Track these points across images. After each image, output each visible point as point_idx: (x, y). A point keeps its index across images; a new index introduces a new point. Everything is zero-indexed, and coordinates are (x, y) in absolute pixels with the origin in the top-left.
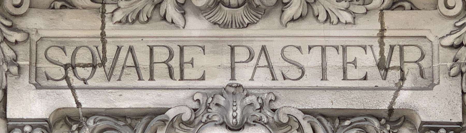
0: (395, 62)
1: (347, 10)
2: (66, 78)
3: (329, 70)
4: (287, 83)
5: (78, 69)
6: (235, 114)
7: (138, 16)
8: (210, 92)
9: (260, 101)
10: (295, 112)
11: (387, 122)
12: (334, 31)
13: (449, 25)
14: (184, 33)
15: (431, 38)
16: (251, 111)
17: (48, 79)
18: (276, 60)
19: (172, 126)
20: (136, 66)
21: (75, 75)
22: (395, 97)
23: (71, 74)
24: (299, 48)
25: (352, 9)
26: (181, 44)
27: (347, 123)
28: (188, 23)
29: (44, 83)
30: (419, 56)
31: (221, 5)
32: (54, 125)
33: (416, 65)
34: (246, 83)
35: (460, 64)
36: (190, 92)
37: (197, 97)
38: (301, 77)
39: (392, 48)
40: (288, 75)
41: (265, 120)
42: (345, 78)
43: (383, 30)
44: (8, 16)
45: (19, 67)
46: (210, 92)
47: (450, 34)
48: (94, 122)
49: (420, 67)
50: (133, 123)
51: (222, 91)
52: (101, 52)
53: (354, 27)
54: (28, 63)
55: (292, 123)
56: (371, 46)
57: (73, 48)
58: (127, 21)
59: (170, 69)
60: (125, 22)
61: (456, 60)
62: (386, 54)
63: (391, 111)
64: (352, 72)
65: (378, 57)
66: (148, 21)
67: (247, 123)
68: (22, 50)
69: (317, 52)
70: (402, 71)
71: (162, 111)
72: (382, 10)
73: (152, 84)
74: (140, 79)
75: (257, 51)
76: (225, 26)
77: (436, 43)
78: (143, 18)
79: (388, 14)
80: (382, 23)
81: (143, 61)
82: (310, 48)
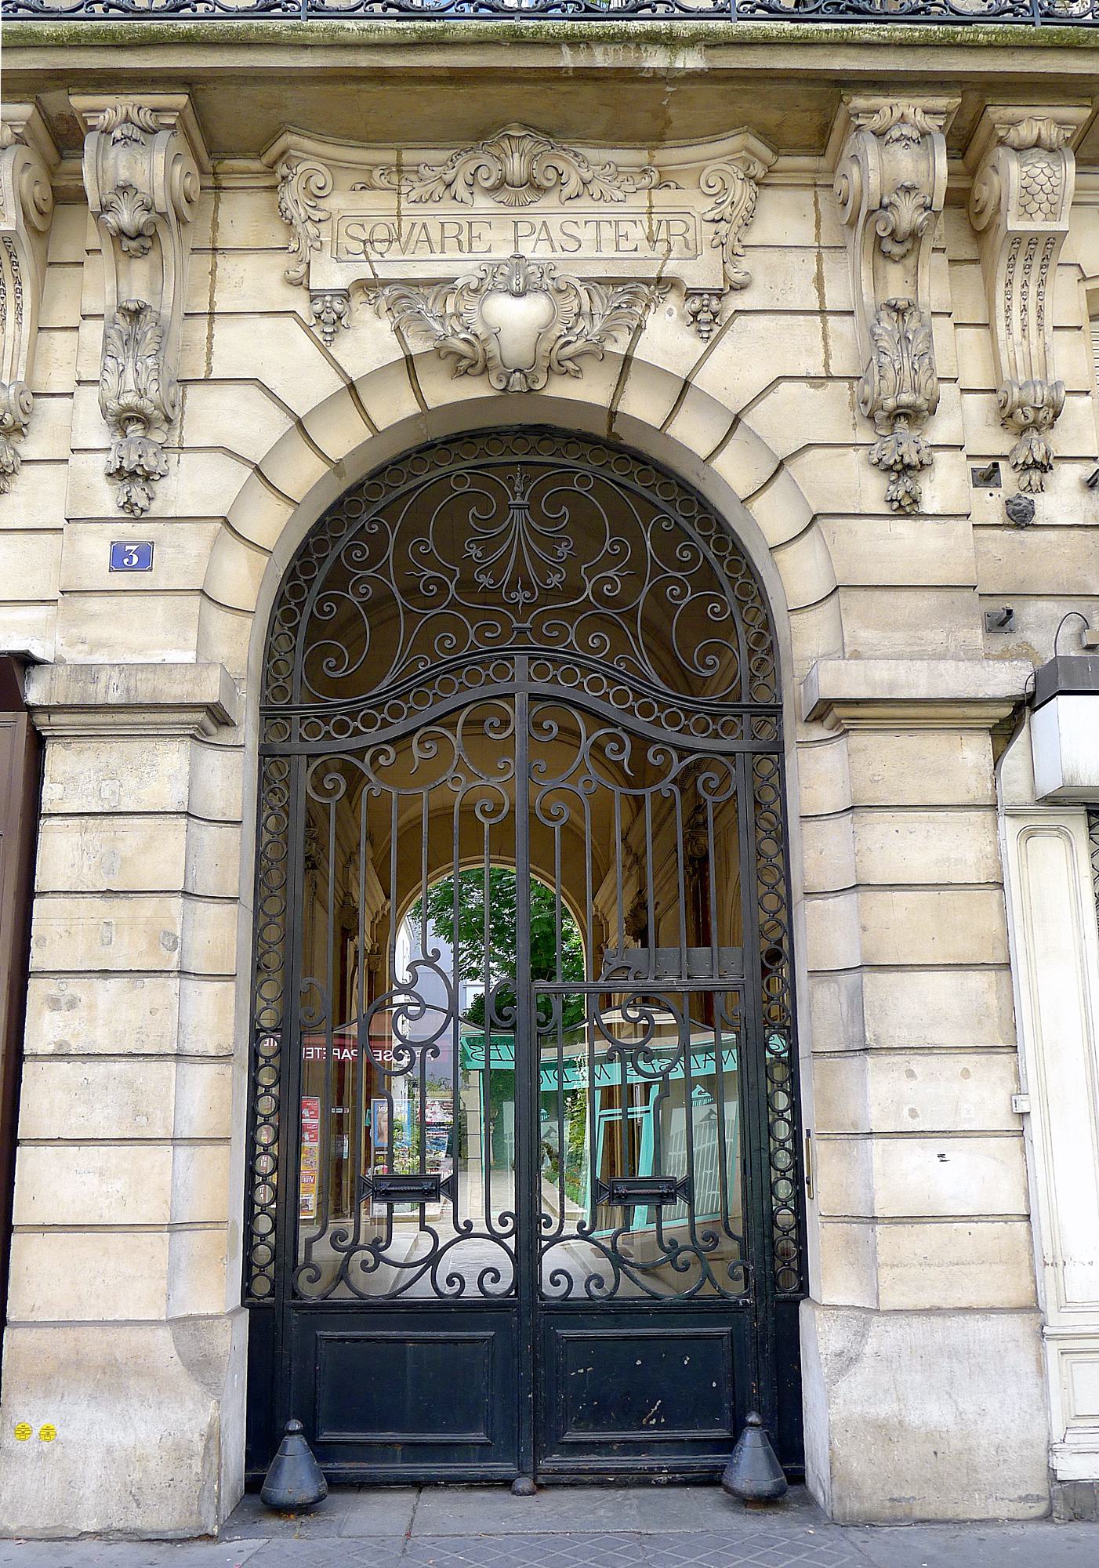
0: (663, 235)
4: (566, 255)
8: (496, 262)
9: (541, 270)
18: (556, 234)
20: (429, 240)
24: (576, 223)
29: (346, 257)
33: (681, 238)
35: (721, 236)
39: (660, 222)
58: (421, 201)
59: (459, 241)
64: (623, 245)
65: (647, 231)
71: (454, 280)
73: (443, 257)
80: (650, 202)
81: (436, 236)
82: (586, 223)
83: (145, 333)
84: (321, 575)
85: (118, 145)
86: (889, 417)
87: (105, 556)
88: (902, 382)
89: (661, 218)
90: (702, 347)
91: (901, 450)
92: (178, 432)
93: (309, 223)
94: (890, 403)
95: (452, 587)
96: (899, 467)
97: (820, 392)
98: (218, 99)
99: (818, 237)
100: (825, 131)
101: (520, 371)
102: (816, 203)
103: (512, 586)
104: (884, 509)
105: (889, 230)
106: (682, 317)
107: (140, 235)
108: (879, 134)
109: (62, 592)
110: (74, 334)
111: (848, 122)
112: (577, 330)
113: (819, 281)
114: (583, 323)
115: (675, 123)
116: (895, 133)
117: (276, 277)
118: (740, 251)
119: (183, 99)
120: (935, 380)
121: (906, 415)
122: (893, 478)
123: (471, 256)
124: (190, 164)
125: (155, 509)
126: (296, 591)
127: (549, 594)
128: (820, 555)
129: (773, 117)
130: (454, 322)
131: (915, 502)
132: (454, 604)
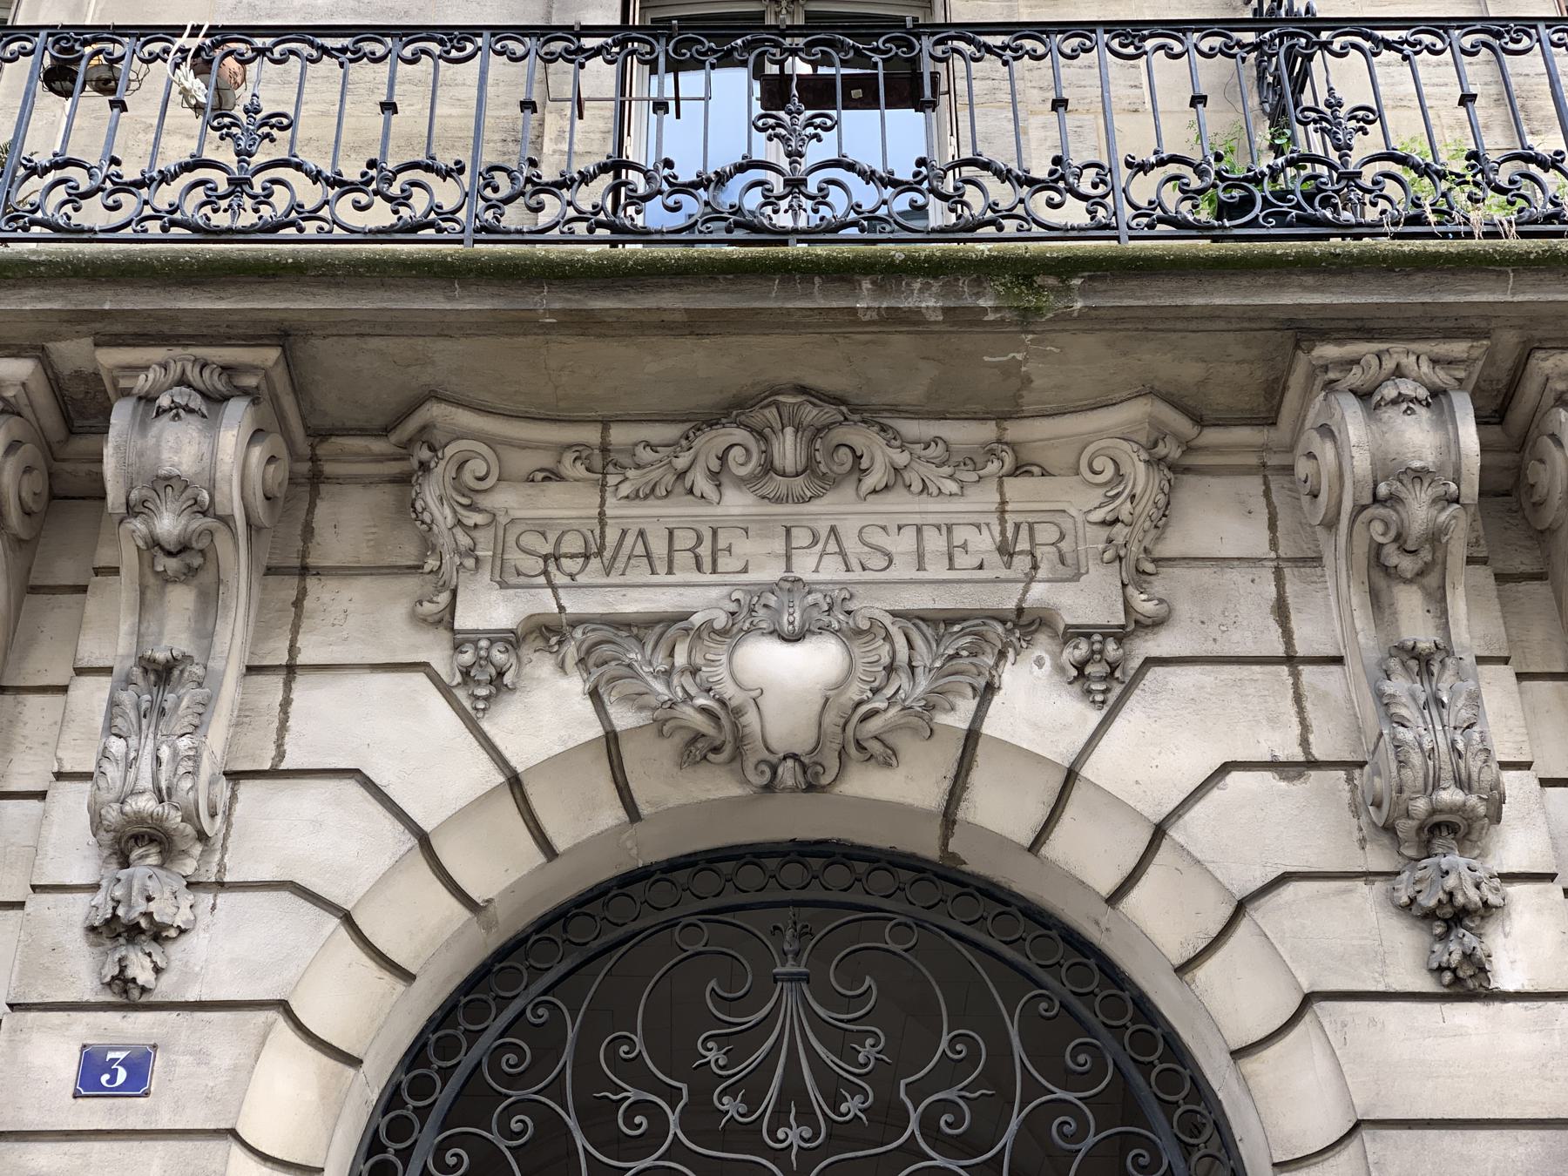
0: (1023, 545)
1: (951, 477)
2: (545, 573)
3: (928, 556)
4: (868, 576)
5: (563, 560)
6: (791, 619)
7: (653, 490)
8: (756, 588)
9: (828, 600)
10: (878, 614)
11: (1016, 625)
12: (933, 505)
13: (1097, 496)
14: (719, 510)
15: (1073, 512)
16: (815, 614)
17: (519, 575)
18: (852, 545)
19: (699, 637)
20: (648, 556)
21: (558, 569)
22: (1026, 591)
23: (552, 568)
24: (884, 528)
25: (958, 475)
26: (714, 526)
27: (957, 628)
28: (725, 498)
30: (1056, 536)
31: (772, 473)
32: (524, 638)
33: (1053, 549)
34: (808, 576)
35: (1117, 546)
36: (725, 590)
37: (735, 596)
38: (888, 567)
39: (1017, 526)
40: (868, 564)
41: (836, 625)
42: (951, 568)
43: (1003, 502)
44: (466, 492)
45: (477, 559)
46: (756, 588)
47: (1100, 507)
48: (584, 633)
49: (1060, 551)
50: (642, 633)
51: (772, 588)
52: (597, 537)
53: (962, 499)
54: (491, 553)
55: (875, 629)
56: (988, 525)
57: (558, 533)
58: (637, 496)
59: (697, 558)
60: (635, 496)
61: (1110, 541)
62: (1009, 534)
63: (1020, 611)
64: (961, 560)
65: (998, 538)
66: (667, 496)
67: (809, 630)
68: (484, 537)
69: (910, 533)
70: (1033, 556)
71: (685, 616)
72: (1000, 477)
74: (653, 573)
75: (824, 533)
76: (778, 500)
77: (1080, 518)
78: (661, 491)
79: (1008, 482)
80: (1002, 494)
81: (659, 547)
82: (900, 528)
83: (180, 699)
84: (444, 1096)
85: (165, 418)
86: (1420, 829)
87: (67, 1067)
88: (1438, 770)
89: (1019, 518)
90: (1095, 717)
91: (1451, 882)
92: (217, 857)
93: (458, 531)
94: (1421, 805)
95: (673, 1118)
96: (1448, 911)
97: (1298, 789)
98: (324, 352)
99: (1274, 544)
100: (1275, 390)
101: (795, 757)
102: (1267, 494)
103: (780, 1118)
104: (1427, 984)
105: (1392, 534)
106: (1060, 669)
107: (183, 548)
108: (1364, 395)
110: (58, 699)
111: (1311, 376)
112: (889, 692)
113: (1281, 612)
114: (902, 680)
115: (1037, 383)
116: (1389, 392)
117: (398, 612)
118: (1149, 567)
119: (271, 355)
120: (1495, 766)
121: (1452, 828)
122: (1438, 931)
124: (274, 442)
125: (165, 989)
126: (400, 1129)
127: (842, 1135)
128: (1322, 1065)
129: (1189, 372)
130: (687, 681)
131: (1483, 970)
132: (676, 1151)
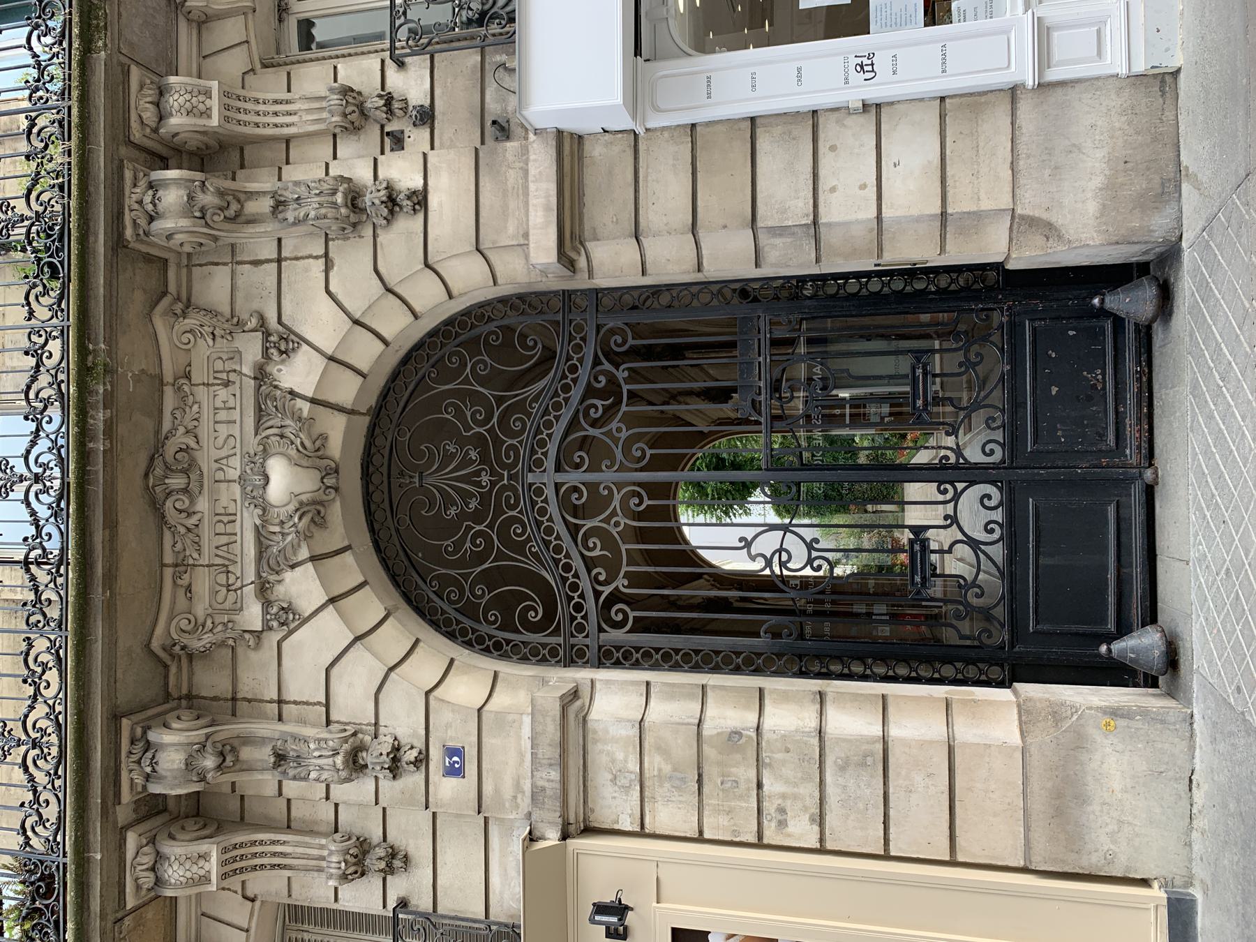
0: (224, 376)
1: (191, 407)
2: (235, 590)
4: (238, 445)
10: (256, 441)
13: (200, 342)
14: (206, 513)
15: (208, 353)
18: (224, 453)
20: (228, 544)
22: (246, 375)
23: (233, 588)
29: (239, 605)
34: (238, 473)
36: (244, 509)
39: (215, 378)
40: (233, 445)
51: (243, 488)
59: (229, 522)
60: (199, 551)
61: (223, 337)
62: (219, 382)
63: (255, 378)
64: (231, 404)
68: (218, 619)
69: (218, 427)
71: (256, 527)
73: (239, 534)
75: (218, 465)
76: (202, 486)
81: (224, 539)
83: (293, 750)
84: (468, 623)
85: (157, 768)
86: (354, 212)
87: (453, 782)
88: (328, 202)
89: (211, 377)
90: (305, 347)
91: (377, 202)
92: (364, 727)
93: (215, 631)
94: (343, 210)
95: (478, 528)
96: (390, 204)
97: (337, 261)
98: (123, 699)
99: (225, 264)
100: (149, 259)
101: (322, 478)
102: (201, 265)
103: (478, 484)
104: (421, 216)
105: (219, 212)
106: (283, 361)
107: (222, 754)
108: (151, 219)
109: (479, 813)
110: (293, 802)
111: (142, 242)
112: (292, 437)
113: (257, 263)
114: (287, 432)
115: (143, 367)
116: (150, 207)
117: (253, 656)
118: (235, 320)
119: (125, 721)
120: (327, 178)
121: (354, 199)
122: (398, 209)
123: (239, 514)
124: (170, 718)
125: (420, 744)
126: (480, 640)
127: (484, 459)
128: (454, 262)
129: (139, 296)
130: (286, 526)
131: (414, 192)
132: (491, 526)
